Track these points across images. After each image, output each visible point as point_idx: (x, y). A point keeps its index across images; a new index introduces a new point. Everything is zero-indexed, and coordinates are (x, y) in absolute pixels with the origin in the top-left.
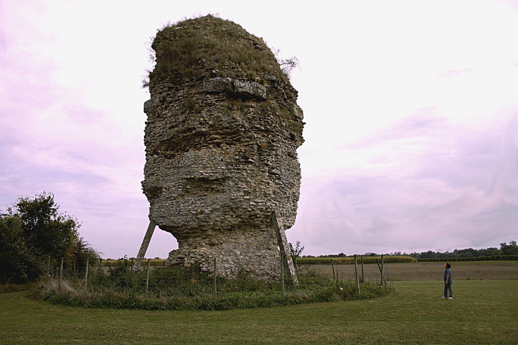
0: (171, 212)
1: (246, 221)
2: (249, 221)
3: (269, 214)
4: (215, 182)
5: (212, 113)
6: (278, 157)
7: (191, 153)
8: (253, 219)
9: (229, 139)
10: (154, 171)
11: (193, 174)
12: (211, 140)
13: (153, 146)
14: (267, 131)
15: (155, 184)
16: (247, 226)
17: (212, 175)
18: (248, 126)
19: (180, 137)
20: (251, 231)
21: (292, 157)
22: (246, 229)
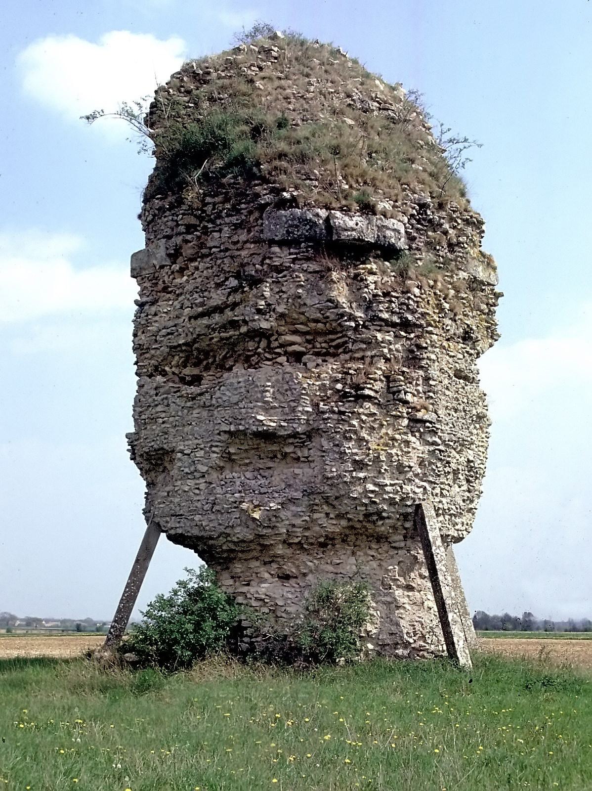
0: (196, 504)
1: (358, 526)
2: (365, 527)
3: (410, 510)
4: (291, 441)
5: (284, 289)
6: (431, 382)
7: (239, 374)
8: (374, 523)
9: (320, 343)
10: (157, 413)
11: (243, 422)
12: (281, 346)
13: (153, 356)
14: (406, 325)
15: (158, 442)
16: (360, 538)
17: (284, 427)
18: (362, 315)
19: (213, 338)
20: (370, 548)
21: (466, 378)
22: (358, 543)
